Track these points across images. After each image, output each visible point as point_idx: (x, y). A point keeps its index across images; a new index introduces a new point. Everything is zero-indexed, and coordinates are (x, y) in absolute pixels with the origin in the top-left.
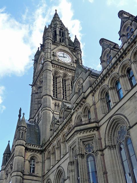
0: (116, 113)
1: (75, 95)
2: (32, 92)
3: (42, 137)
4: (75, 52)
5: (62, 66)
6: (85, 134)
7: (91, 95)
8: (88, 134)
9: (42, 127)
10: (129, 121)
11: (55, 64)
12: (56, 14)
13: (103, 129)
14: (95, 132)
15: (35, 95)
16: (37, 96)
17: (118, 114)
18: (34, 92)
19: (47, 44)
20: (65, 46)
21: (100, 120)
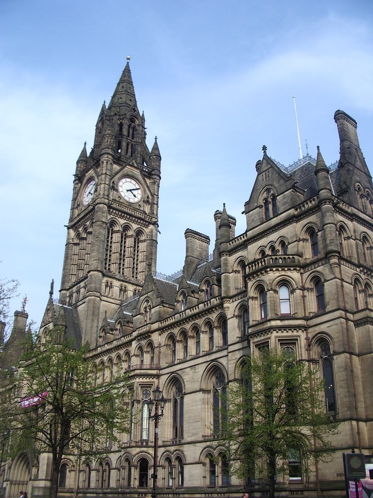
0: (177, 372)
1: (139, 316)
2: (68, 239)
3: (85, 337)
4: (149, 178)
5: (125, 213)
6: (144, 380)
7: (157, 333)
8: (148, 380)
9: (85, 322)
10: (186, 387)
11: (114, 209)
12: (127, 71)
13: (164, 379)
14: (155, 380)
15: (72, 247)
16: (76, 249)
17: (177, 374)
18: (71, 241)
19: (105, 164)
20: (135, 167)
21: (163, 367)
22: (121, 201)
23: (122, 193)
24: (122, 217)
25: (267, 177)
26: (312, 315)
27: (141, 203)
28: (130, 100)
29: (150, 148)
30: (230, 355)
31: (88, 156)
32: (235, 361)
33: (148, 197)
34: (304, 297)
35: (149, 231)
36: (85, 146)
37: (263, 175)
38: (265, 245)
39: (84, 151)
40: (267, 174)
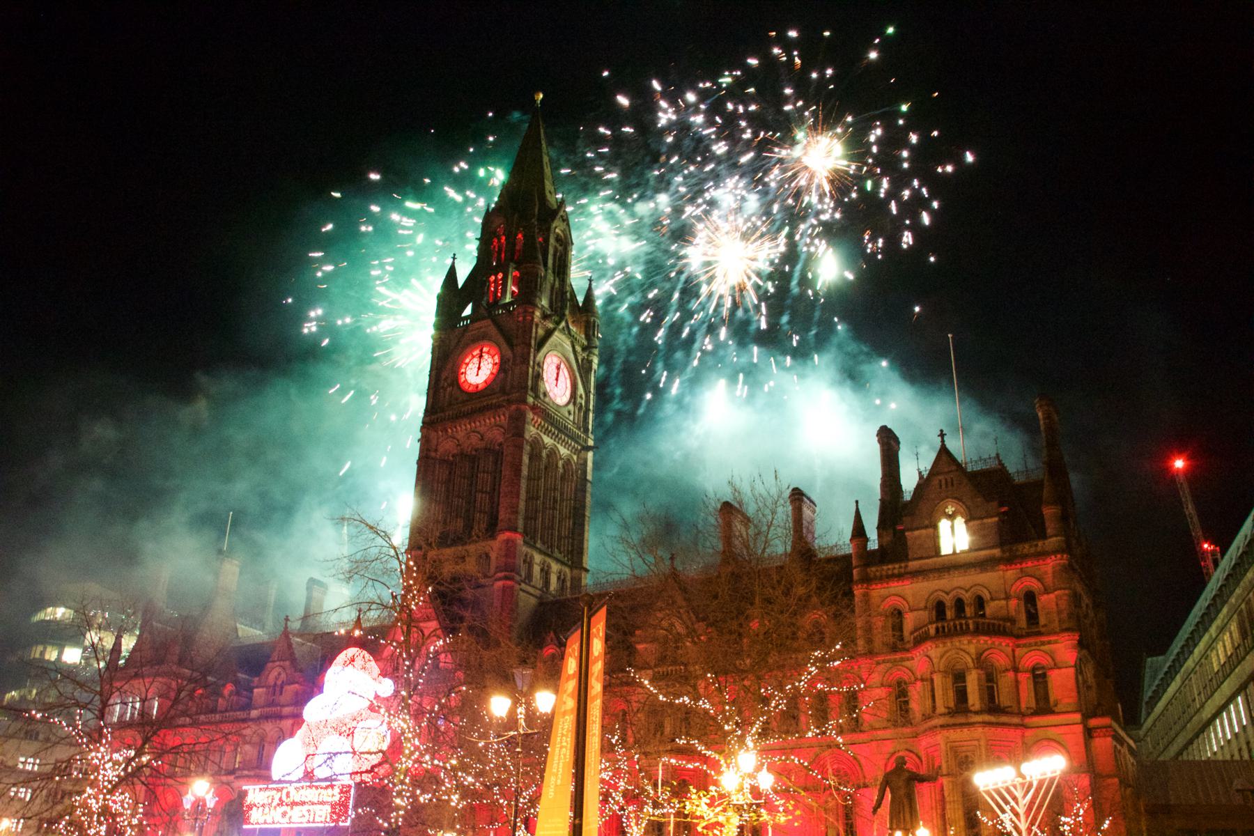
22: (547, 400)
23: (547, 385)
24: (547, 432)
25: (950, 484)
26: (1030, 711)
27: (571, 407)
28: (550, 192)
29: (580, 299)
30: (874, 744)
31: (460, 286)
32: (887, 756)
33: (581, 397)
34: (1017, 682)
35: (582, 462)
36: (453, 263)
37: (940, 481)
38: (946, 590)
39: (452, 274)
40: (949, 480)
